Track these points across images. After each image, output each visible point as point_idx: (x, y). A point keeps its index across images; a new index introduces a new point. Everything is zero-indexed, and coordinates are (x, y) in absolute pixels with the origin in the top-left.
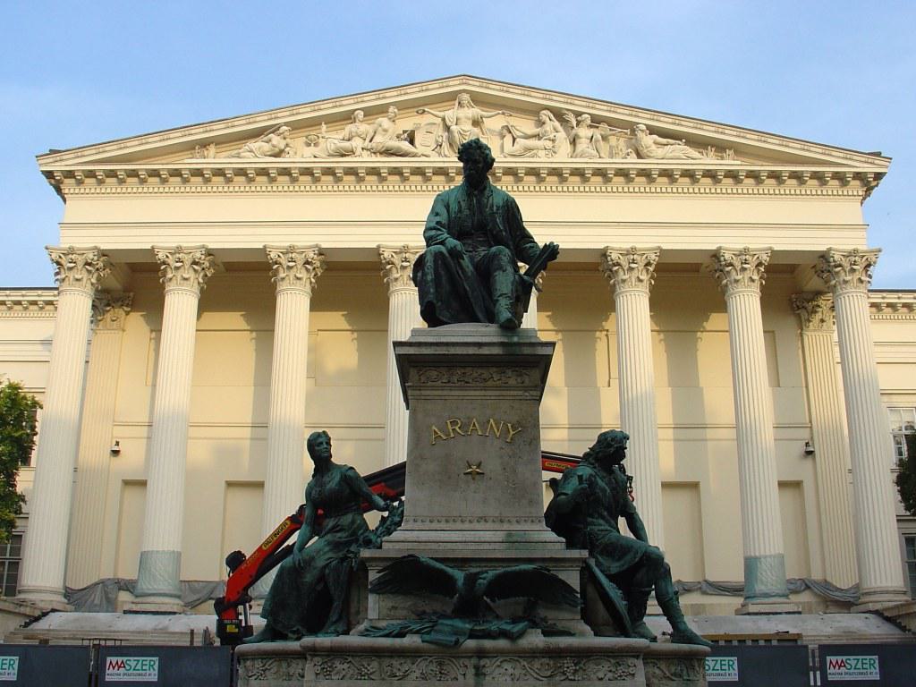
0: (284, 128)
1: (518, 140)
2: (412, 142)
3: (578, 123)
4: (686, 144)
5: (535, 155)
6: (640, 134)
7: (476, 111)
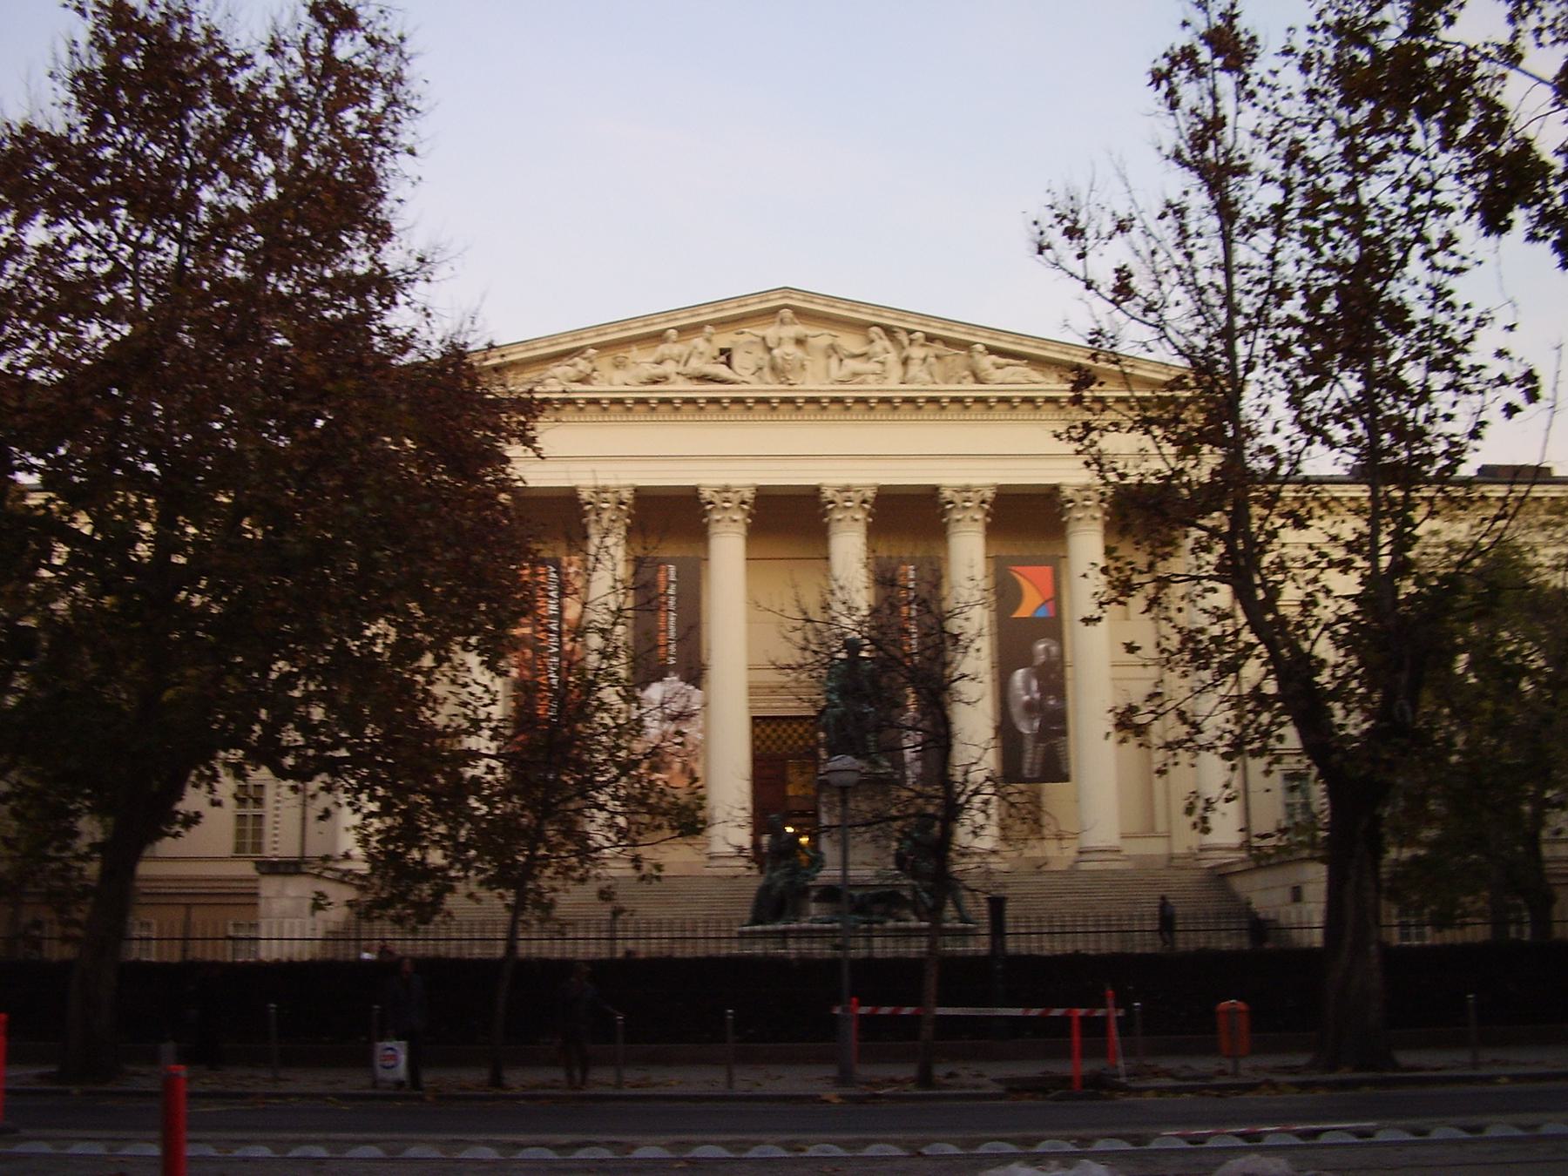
0: (592, 351)
1: (846, 361)
2: (728, 363)
3: (911, 341)
6: (977, 357)
7: (799, 329)
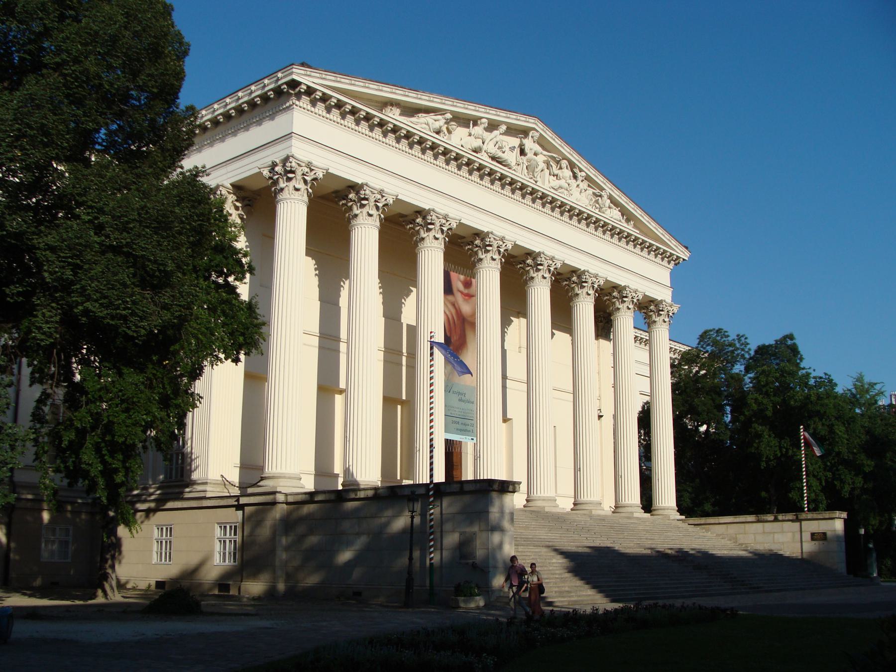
4: (619, 211)
5: (562, 193)
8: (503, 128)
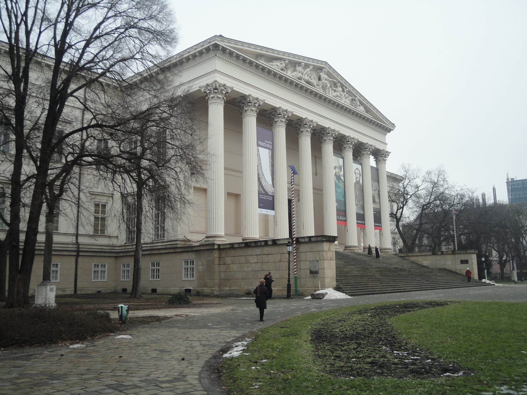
8: (312, 67)
